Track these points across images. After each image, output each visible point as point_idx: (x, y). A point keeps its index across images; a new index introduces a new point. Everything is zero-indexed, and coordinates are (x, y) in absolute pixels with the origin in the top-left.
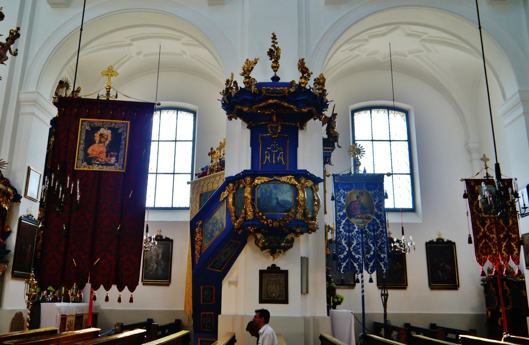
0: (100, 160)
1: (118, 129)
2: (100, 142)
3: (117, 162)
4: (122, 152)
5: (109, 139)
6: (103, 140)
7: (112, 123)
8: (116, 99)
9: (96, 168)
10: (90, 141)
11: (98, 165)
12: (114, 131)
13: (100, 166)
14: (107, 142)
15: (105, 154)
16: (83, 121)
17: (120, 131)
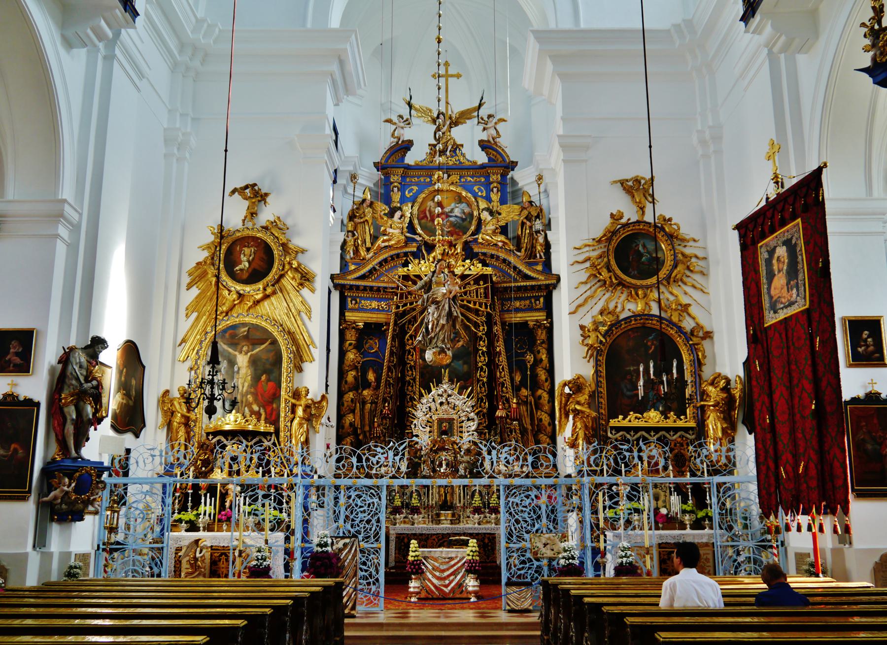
0: (783, 300)
1: (792, 238)
2: (779, 271)
3: (798, 295)
4: (800, 276)
5: (786, 261)
6: (781, 265)
7: (784, 232)
8: (784, 190)
9: (782, 315)
10: (771, 276)
11: (782, 308)
12: (787, 243)
13: (785, 310)
14: (785, 268)
15: (786, 288)
16: (761, 247)
17: (793, 242)
